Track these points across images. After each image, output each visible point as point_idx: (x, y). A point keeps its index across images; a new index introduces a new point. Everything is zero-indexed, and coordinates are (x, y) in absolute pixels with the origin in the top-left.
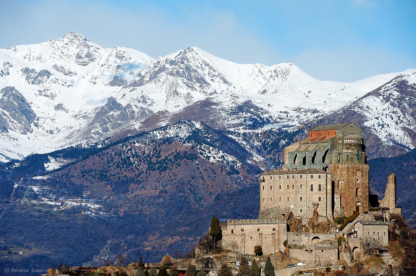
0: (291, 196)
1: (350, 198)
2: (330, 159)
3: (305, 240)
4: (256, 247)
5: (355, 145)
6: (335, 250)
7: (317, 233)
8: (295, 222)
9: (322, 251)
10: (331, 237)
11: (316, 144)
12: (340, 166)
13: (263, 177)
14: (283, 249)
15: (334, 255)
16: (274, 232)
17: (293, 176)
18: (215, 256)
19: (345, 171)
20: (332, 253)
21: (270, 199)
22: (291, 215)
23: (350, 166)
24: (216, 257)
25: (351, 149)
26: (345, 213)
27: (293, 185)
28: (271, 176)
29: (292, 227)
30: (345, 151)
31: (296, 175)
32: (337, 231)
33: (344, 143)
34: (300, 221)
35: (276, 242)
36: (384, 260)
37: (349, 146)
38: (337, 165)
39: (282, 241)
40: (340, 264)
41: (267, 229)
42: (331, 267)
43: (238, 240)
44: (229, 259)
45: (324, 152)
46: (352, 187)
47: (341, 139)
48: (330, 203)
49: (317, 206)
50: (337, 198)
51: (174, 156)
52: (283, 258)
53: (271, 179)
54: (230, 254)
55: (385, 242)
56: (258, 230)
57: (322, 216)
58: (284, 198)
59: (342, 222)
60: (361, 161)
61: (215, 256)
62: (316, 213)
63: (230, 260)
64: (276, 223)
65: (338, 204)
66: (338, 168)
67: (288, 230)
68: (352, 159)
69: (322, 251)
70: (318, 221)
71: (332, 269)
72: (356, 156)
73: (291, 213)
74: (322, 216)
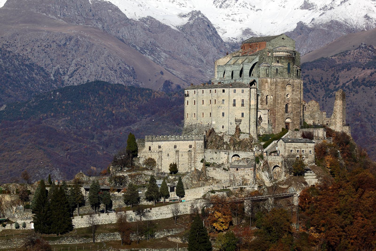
0: (214, 111)
1: (279, 114)
2: (259, 73)
3: (222, 157)
4: (171, 165)
5: (285, 58)
7: (238, 150)
8: (216, 139)
9: (237, 170)
10: (250, 155)
11: (246, 57)
12: (269, 80)
14: (200, 166)
16: (191, 149)
17: (215, 90)
18: (129, 174)
19: (273, 85)
21: (194, 114)
22: (212, 132)
23: (279, 80)
25: (280, 62)
26: (273, 130)
27: (215, 100)
28: (195, 90)
29: (209, 144)
30: (274, 64)
31: (218, 89)
33: (274, 56)
34: (221, 138)
35: (192, 159)
36: (306, 180)
37: (279, 59)
38: (265, 79)
39: (199, 159)
40: (256, 184)
41: (183, 145)
42: (246, 186)
43: (155, 157)
44: (144, 177)
45: (251, 65)
46: (281, 103)
47: (271, 52)
48: (253, 119)
49: (239, 123)
50: (265, 114)
51: (352, 82)
52: (199, 177)
53: (195, 93)
54: (146, 172)
55: (309, 160)
56: (175, 147)
57: (244, 133)
58: (207, 114)
60: (292, 75)
61: (129, 174)
62: (238, 130)
63: (146, 178)
64: (192, 140)
66: (267, 82)
67: (206, 146)
69: (237, 170)
70: (240, 138)
71: (247, 189)
72: (286, 70)
73: (213, 129)
74: (244, 133)
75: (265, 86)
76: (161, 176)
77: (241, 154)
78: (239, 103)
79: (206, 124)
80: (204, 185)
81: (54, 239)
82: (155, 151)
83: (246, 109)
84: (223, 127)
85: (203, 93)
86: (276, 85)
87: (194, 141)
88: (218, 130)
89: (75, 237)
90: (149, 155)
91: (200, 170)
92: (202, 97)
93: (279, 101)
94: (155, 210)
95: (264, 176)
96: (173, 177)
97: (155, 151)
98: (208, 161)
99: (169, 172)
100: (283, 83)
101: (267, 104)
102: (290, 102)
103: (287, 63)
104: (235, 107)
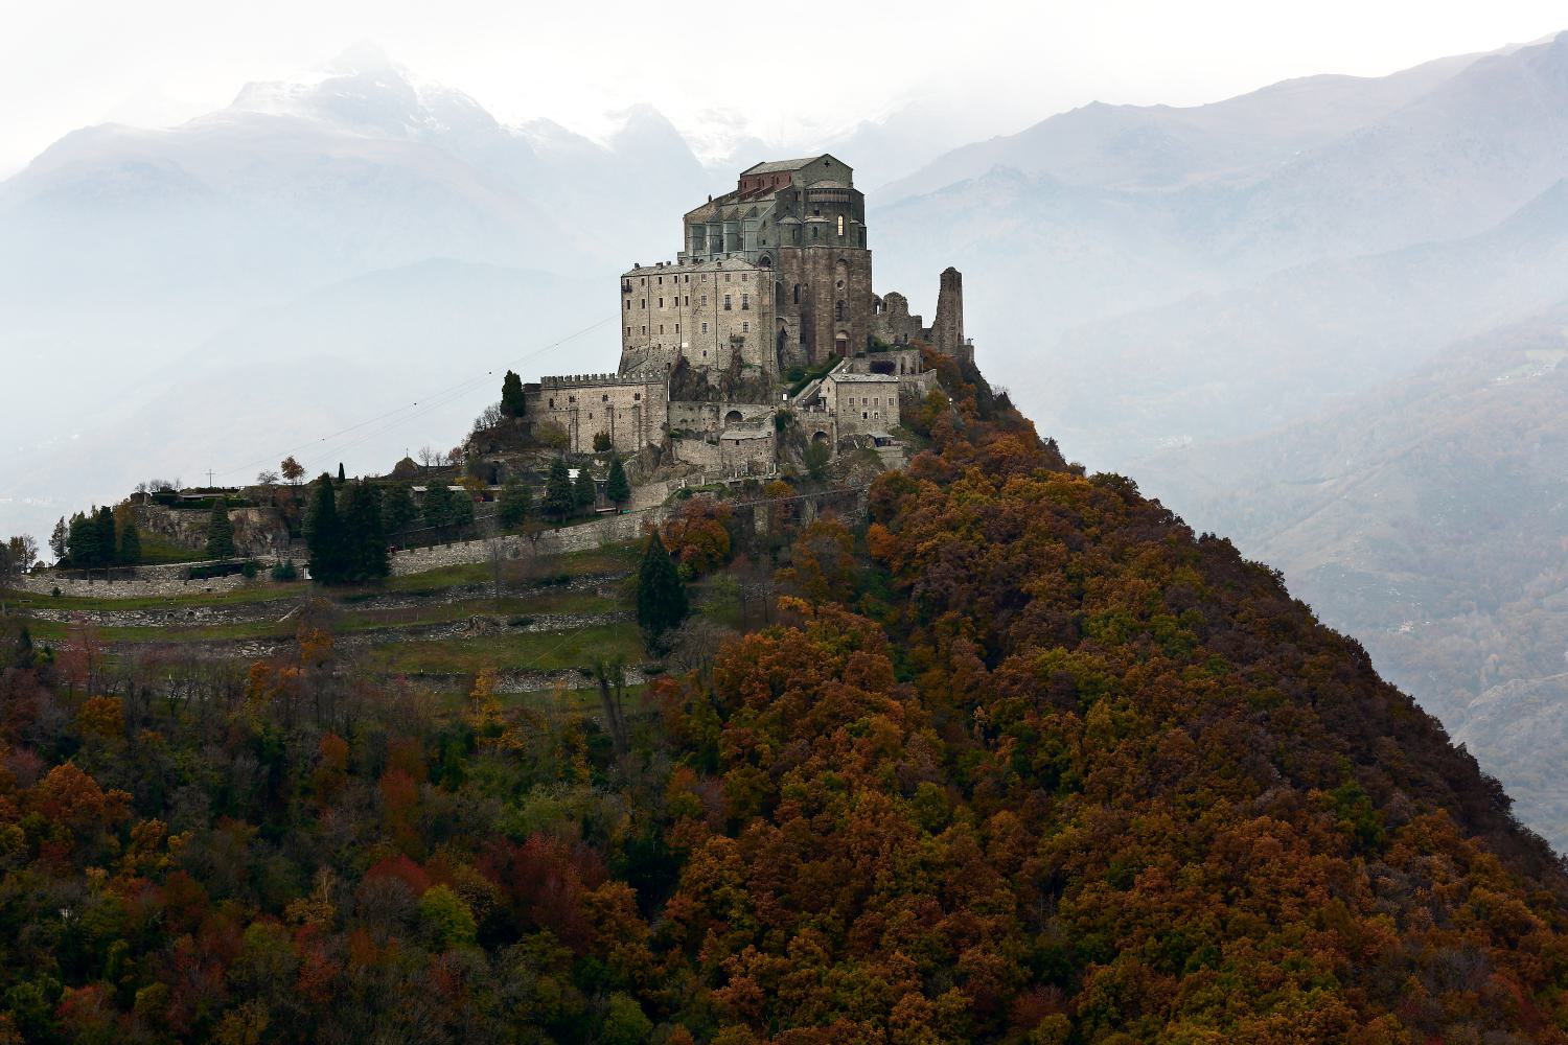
0: (686, 322)
4: (597, 437)
9: (737, 443)
14: (658, 437)
24: (512, 462)
32: (785, 397)
34: (703, 378)
35: (642, 424)
36: (883, 461)
41: (623, 397)
43: (565, 420)
52: (657, 462)
56: (605, 398)
58: (669, 327)
59: (798, 378)
62: (738, 362)
66: (795, 256)
69: (737, 443)
75: (791, 265)
76: (580, 460)
77: (744, 411)
78: (736, 306)
79: (667, 347)
80: (666, 477)
81: (356, 600)
84: (705, 355)
86: (814, 263)
87: (644, 387)
88: (696, 360)
89: (400, 595)
90: (550, 417)
91: (659, 445)
94: (567, 532)
95: (793, 454)
96: (603, 463)
98: (675, 425)
99: (593, 451)
100: (830, 256)
101: (796, 302)
102: (846, 296)
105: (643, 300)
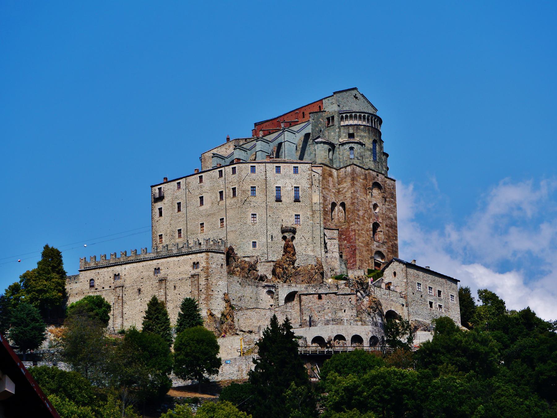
0: (231, 213)
1: (361, 240)
2: (312, 155)
6: (349, 296)
9: (320, 297)
13: (160, 189)
15: (347, 309)
20: (343, 304)
25: (358, 136)
39: (216, 293)
56: (157, 270)
62: (289, 250)
65: (334, 250)
68: (362, 156)
69: (320, 297)
70: (296, 265)
72: (370, 153)
78: (288, 196)
82: (107, 288)
83: (306, 206)
84: (254, 244)
85: (201, 181)
87: (203, 254)
92: (197, 193)
93: (361, 213)
97: (107, 288)
103: (371, 141)
104: (280, 203)
105: (179, 204)
